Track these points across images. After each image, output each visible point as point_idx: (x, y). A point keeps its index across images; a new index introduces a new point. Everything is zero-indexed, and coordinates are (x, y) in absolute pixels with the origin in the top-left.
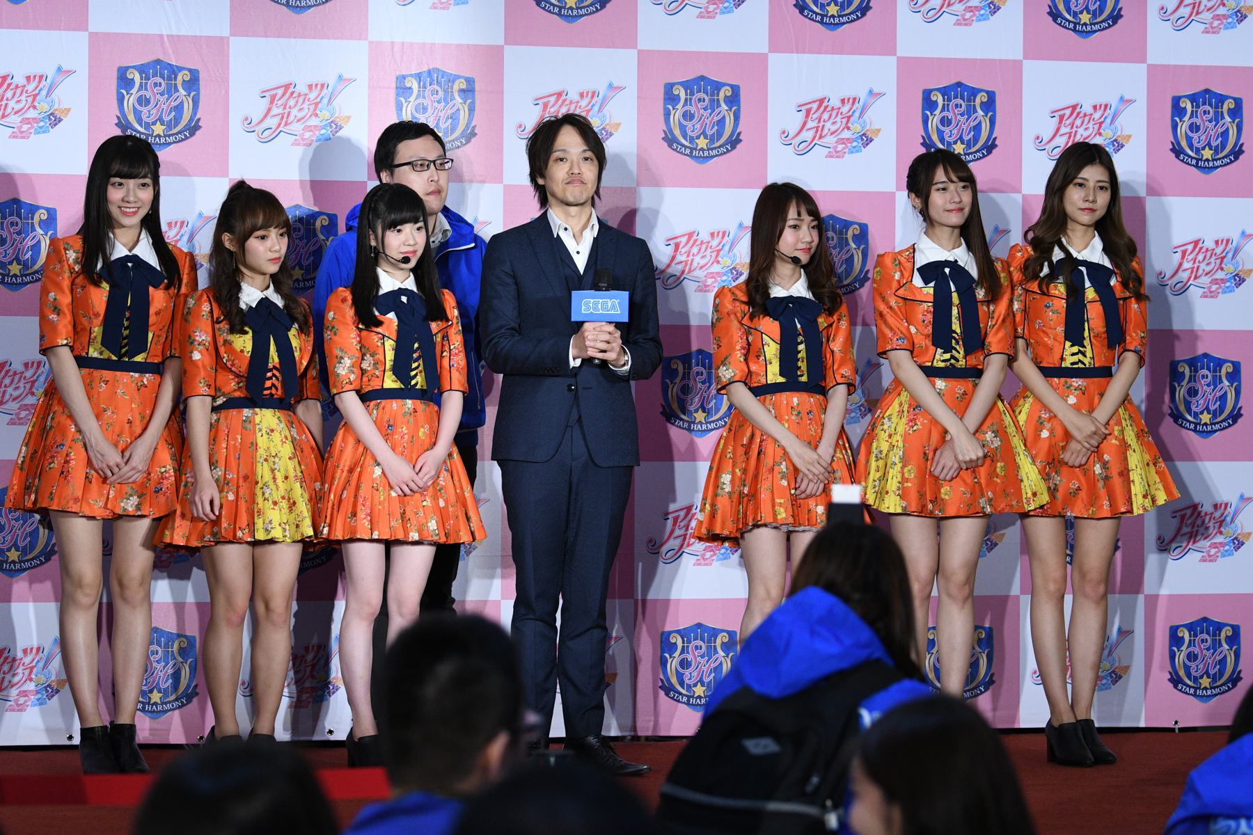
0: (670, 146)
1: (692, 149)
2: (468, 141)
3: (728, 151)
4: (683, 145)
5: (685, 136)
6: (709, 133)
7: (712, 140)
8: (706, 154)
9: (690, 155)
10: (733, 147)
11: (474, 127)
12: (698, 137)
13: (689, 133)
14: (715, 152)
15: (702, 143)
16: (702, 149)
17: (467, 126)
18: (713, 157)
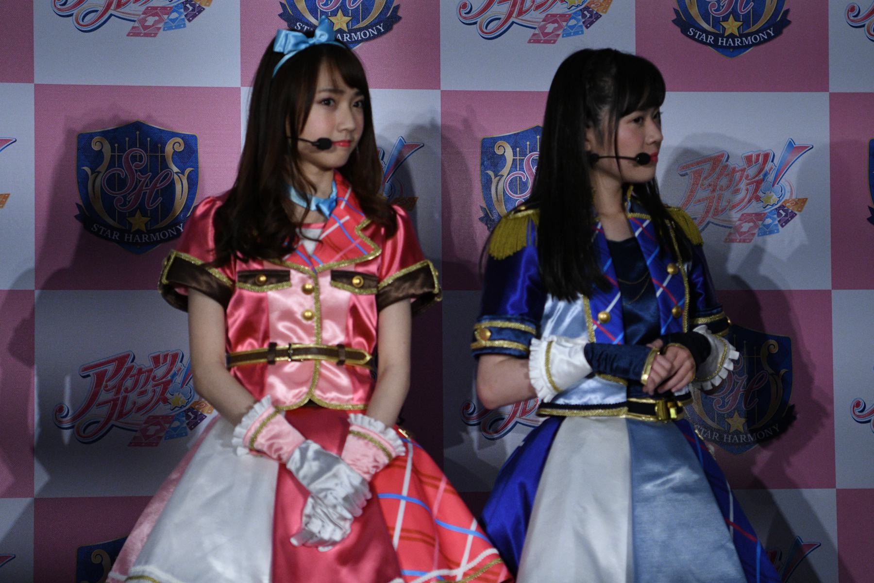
0: (685, 31)
1: (716, 36)
2: (388, 28)
3: (770, 38)
4: (704, 31)
5: (706, 17)
6: (742, 12)
7: (746, 21)
8: (738, 42)
9: (715, 45)
10: (778, 32)
11: (397, 8)
12: (726, 19)
13: (712, 12)
14: (751, 40)
15: (732, 26)
16: (732, 36)
17: (387, 7)
18: (749, 46)
